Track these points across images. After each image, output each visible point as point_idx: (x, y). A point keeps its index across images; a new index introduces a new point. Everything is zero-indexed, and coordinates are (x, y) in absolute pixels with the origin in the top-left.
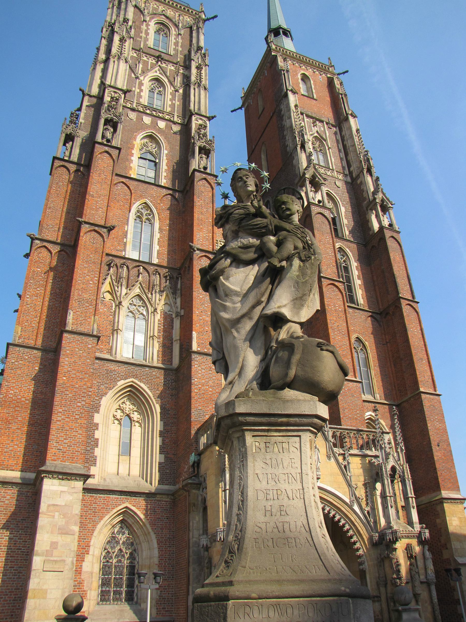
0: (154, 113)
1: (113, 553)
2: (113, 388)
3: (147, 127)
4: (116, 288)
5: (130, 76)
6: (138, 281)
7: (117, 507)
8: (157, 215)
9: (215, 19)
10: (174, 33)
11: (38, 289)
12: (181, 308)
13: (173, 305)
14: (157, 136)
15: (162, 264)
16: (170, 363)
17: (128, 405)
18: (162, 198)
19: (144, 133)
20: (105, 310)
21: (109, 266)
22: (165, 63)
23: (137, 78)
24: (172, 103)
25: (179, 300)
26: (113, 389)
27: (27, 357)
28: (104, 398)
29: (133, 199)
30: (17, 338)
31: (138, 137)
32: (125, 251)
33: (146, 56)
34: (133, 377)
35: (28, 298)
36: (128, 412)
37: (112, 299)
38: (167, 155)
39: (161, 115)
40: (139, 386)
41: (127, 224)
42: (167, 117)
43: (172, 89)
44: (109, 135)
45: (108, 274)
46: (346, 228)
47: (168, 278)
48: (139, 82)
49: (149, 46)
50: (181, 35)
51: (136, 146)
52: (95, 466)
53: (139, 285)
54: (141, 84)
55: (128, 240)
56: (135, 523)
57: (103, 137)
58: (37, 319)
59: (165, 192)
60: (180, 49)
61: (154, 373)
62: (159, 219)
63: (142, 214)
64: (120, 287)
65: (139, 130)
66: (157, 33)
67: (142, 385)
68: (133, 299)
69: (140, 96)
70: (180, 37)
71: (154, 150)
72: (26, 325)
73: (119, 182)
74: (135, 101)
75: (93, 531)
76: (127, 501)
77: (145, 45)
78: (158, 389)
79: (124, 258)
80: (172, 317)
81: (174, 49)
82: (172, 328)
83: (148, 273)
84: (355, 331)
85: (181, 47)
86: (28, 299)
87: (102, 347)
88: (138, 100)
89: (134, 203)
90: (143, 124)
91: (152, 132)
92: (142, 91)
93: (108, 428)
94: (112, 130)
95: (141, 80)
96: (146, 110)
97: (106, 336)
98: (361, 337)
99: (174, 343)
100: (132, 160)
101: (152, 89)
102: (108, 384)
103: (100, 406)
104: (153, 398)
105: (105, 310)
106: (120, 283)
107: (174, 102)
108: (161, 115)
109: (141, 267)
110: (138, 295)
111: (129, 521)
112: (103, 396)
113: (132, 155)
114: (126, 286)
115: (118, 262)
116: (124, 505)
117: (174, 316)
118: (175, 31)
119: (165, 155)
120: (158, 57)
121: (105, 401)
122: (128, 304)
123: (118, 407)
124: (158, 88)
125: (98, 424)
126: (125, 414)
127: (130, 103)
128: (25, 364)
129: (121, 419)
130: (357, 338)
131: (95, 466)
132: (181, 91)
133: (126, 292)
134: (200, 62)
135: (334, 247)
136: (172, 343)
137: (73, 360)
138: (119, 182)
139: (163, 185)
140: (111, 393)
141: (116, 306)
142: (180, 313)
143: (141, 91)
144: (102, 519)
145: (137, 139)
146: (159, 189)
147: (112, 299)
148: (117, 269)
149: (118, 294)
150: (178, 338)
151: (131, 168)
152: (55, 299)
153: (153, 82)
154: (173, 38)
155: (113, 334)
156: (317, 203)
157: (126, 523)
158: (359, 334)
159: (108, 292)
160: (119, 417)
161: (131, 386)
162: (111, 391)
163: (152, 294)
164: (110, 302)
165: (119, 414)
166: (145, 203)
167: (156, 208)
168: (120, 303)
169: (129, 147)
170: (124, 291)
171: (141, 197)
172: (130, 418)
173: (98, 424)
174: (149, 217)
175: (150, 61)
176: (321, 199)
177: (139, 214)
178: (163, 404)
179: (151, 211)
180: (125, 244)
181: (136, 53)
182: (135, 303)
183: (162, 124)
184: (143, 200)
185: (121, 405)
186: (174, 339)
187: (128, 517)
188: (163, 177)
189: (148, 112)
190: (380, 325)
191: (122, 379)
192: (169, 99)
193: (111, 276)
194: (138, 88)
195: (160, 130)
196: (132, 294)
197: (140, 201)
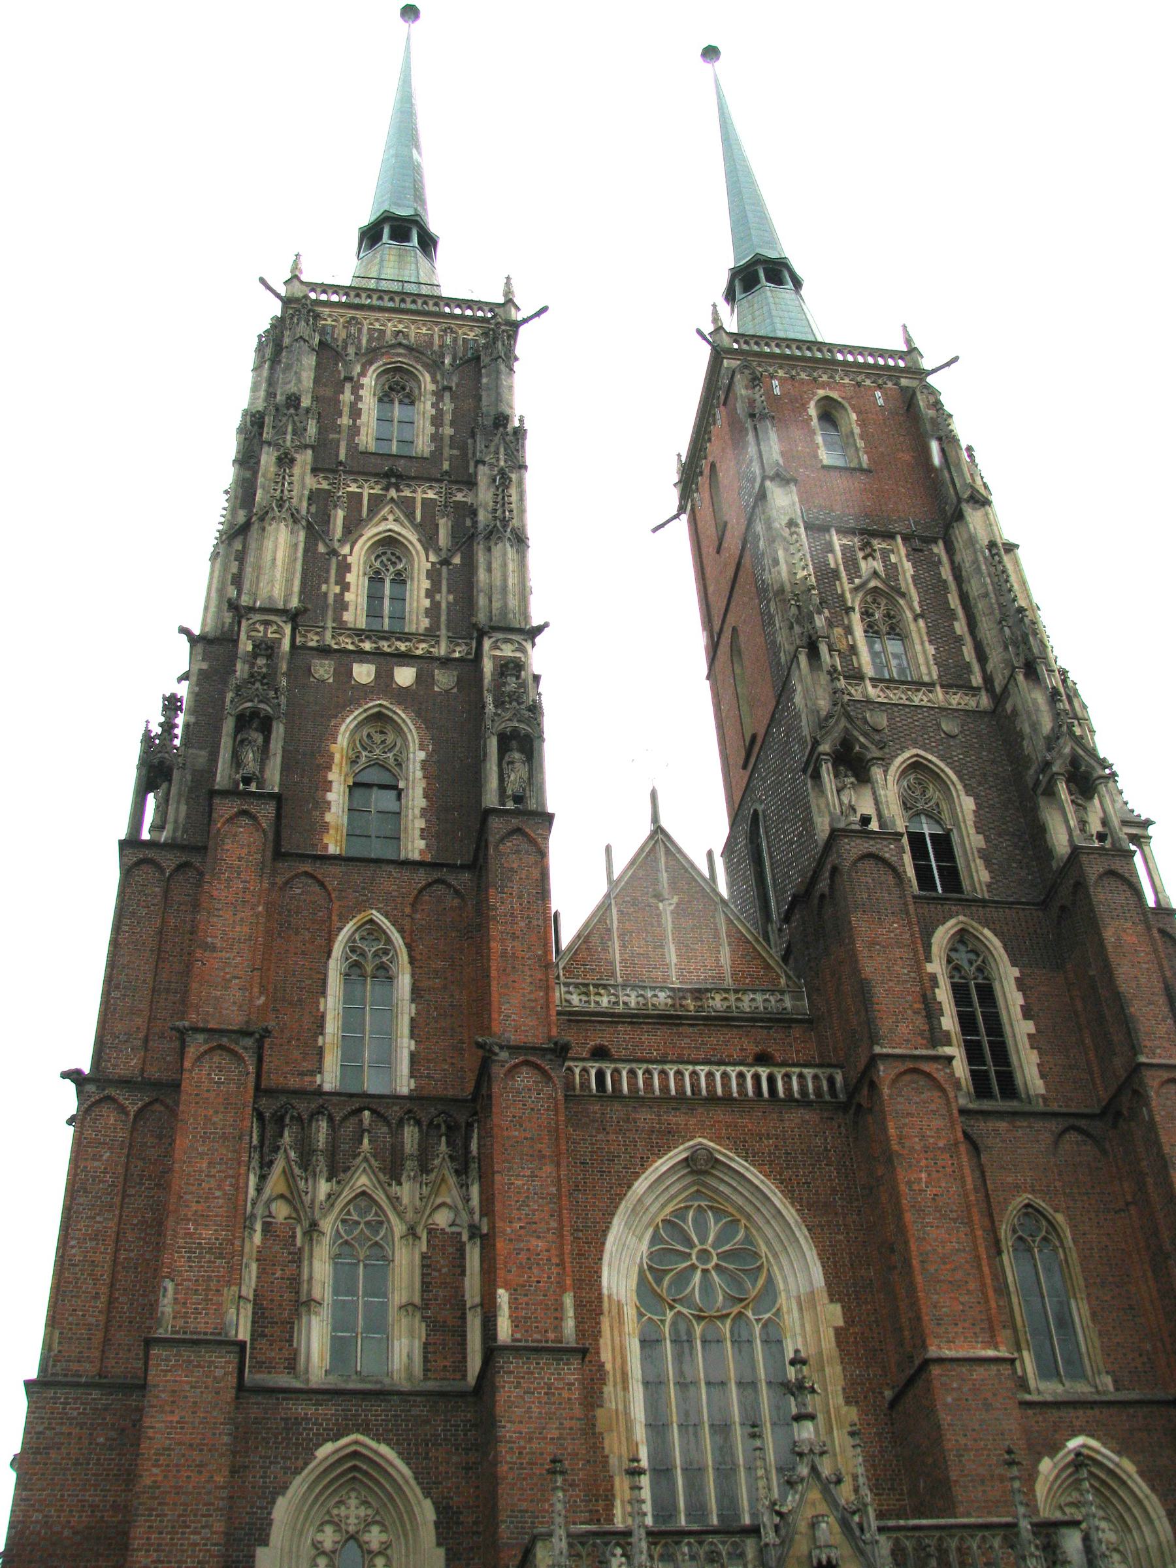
0: (385, 646)
2: (303, 1469)
3: (365, 691)
4: (302, 1184)
5: (310, 549)
6: (359, 1153)
9: (543, 316)
10: (431, 387)
11: (98, 1219)
12: (482, 1215)
13: (460, 1206)
14: (395, 713)
15: (425, 1093)
16: (458, 1375)
18: (416, 897)
19: (356, 713)
20: (277, 1248)
21: (279, 1121)
22: (409, 486)
23: (334, 553)
24: (432, 602)
25: (475, 1190)
26: (306, 1472)
27: (75, 1413)
29: (335, 918)
30: (51, 1363)
31: (343, 727)
32: (320, 1070)
33: (355, 481)
34: (358, 1431)
35: (73, 1247)
36: (352, 1529)
37: (294, 1215)
38: (423, 762)
40: (376, 1452)
42: (421, 649)
43: (432, 558)
45: (278, 1148)
47: (443, 1129)
48: (339, 565)
49: (361, 448)
50: (449, 388)
53: (365, 1165)
54: (344, 567)
55: (329, 1039)
58: (101, 1304)
59: (422, 877)
60: (448, 431)
61: (415, 1411)
62: (412, 960)
63: (363, 954)
64: (310, 1182)
66: (386, 399)
67: (384, 1449)
68: (351, 1207)
69: (342, 605)
70: (447, 395)
71: (390, 755)
72: (71, 1324)
73: (297, 876)
74: (330, 624)
77: (352, 448)
78: (427, 1454)
79: (319, 1092)
80: (460, 1241)
81: (436, 438)
82: (463, 1273)
83: (389, 1124)
84: (1018, 1188)
85: (452, 424)
86: (74, 1251)
87: (273, 1354)
88: (338, 619)
89: (340, 929)
91: (380, 705)
92: (348, 590)
95: (345, 556)
96: (362, 641)
97: (282, 1323)
98: (1041, 1203)
99: (469, 1316)
100: (329, 803)
101: (377, 572)
102: (290, 1458)
103: (270, 1524)
104: (413, 1482)
105: (277, 1248)
106: (311, 1168)
107: (438, 597)
108: (403, 647)
109: (367, 1113)
110: (363, 1193)
112: (278, 1494)
113: (328, 786)
114: (325, 1174)
115: (303, 1107)
117: (465, 1238)
118: (434, 381)
119: (418, 767)
120: (386, 475)
121: (282, 1510)
122: (339, 1223)
124: (394, 564)
126: (345, 1536)
127: (317, 633)
128: (70, 1434)
129: (334, 1552)
130: (1028, 1206)
132: (457, 560)
133: (328, 1191)
134: (502, 463)
136: (463, 1317)
138: (297, 876)
139: (416, 856)
140: (298, 1485)
141: (304, 1234)
142: (479, 1228)
143: (346, 587)
145: (340, 738)
146: (407, 873)
147: (294, 1215)
148: (303, 1129)
149: (307, 1199)
150: (477, 1300)
151: (325, 827)
152: (144, 1239)
153: (380, 550)
154: (429, 404)
155: (299, 1317)
158: (1033, 1192)
160: (328, 1545)
161: (355, 1454)
162: (299, 1479)
163: (400, 1184)
164: (287, 1224)
167: (401, 931)
168: (314, 1225)
169: (318, 766)
171: (360, 907)
172: (360, 1546)
174: (384, 959)
175: (366, 493)
178: (443, 1498)
179: (389, 941)
180: (320, 1052)
181: (326, 478)
182: (356, 1218)
183: (405, 676)
184: (363, 914)
186: (468, 1305)
189: (367, 646)
190: (1104, 1152)
191: (326, 1441)
192: (423, 593)
193: (285, 1150)
194: (337, 583)
195: (402, 696)
196: (347, 1195)
197: (355, 920)
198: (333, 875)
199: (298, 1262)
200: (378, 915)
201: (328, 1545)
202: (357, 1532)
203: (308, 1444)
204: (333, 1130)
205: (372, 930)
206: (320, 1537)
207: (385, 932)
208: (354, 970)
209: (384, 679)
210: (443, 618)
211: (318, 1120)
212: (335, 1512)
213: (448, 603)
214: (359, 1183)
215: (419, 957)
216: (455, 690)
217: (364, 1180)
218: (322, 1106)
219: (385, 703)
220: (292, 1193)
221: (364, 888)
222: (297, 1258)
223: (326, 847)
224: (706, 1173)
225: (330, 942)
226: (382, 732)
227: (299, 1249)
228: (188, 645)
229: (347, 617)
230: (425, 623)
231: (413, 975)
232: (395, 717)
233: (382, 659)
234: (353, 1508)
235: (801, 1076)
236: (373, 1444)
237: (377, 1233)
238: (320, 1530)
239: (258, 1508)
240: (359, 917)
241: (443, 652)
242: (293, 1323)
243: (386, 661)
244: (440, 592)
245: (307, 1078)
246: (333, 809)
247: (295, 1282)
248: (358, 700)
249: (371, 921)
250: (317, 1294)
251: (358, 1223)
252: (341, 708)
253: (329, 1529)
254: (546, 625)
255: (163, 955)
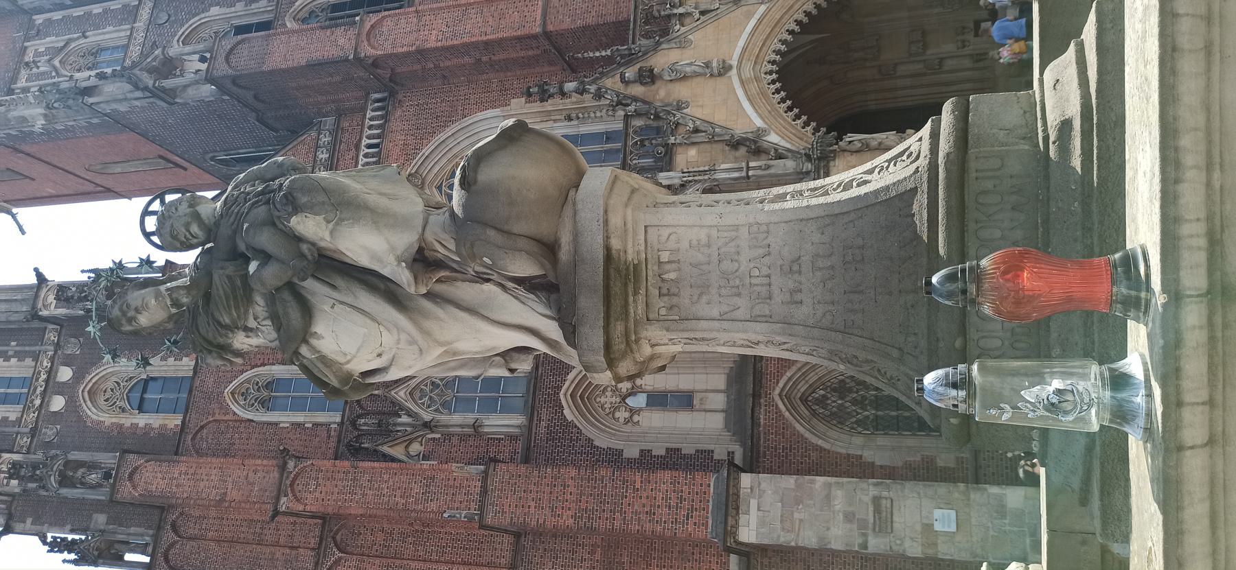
1: (858, 414)
2: (579, 429)
3: (72, 403)
7: (780, 411)
8: (255, 370)
17: (606, 400)
19: (85, 408)
28: (596, 443)
29: (227, 417)
31: (94, 417)
32: (328, 425)
34: (558, 394)
36: (618, 400)
37: (420, 439)
39: (43, 377)
41: (276, 424)
42: (46, 363)
44: (94, 477)
45: (375, 450)
46: (253, 6)
51: (114, 420)
52: (712, 451)
53: (393, 393)
56: (807, 379)
57: (99, 486)
62: (263, 365)
65: (80, 417)
74: (16, 429)
75: (821, 449)
76: (770, 394)
79: (341, 424)
88: (14, 424)
89: (235, 414)
90: (66, 411)
91: (83, 391)
93: (647, 433)
94: (82, 470)
96: (34, 406)
107: (10, 353)
111: (802, 390)
116: (777, 399)
121: (602, 441)
123: (611, 416)
125: (642, 451)
129: (631, 410)
131: (712, 451)
135: (294, 32)
137: (533, 504)
141: (433, 432)
144: (802, 436)
147: (420, 439)
148: (364, 435)
156: (206, 64)
157: (807, 395)
159: (407, 447)
160: (627, 415)
165: (622, 415)
166: (233, 393)
169: (119, 433)
170: (404, 419)
173: (642, 451)
176: (197, 57)
177: (256, 404)
179: (248, 381)
180: (316, 425)
183: (65, 374)
184: (227, 398)
185: (607, 410)
187: (796, 390)
188: (178, 363)
191: (563, 413)
195: (78, 377)
197: (230, 404)
198: (195, 420)
199: (450, 435)
200: (229, 388)
201: (627, 415)
202: (621, 396)
203: (564, 426)
204: (368, 414)
205: (241, 394)
206: (622, 420)
207: (242, 383)
208: (267, 404)
209: (64, 389)
210: (27, 348)
211: (360, 425)
212: (607, 410)
213: (17, 345)
214: (403, 396)
215: (261, 361)
216: (81, 339)
217: (402, 393)
218: (351, 422)
219: (82, 388)
220: (405, 441)
221: (209, 399)
222: (448, 437)
223: (176, 426)
224: (424, 180)
225: (242, 421)
226: (105, 391)
227: (442, 435)
228: (11, 535)
229: (13, 417)
230: (29, 362)
231: (273, 364)
232: (94, 381)
233: (49, 391)
234: (606, 400)
235: (371, 119)
236: (567, 384)
237: (439, 385)
238: (617, 420)
239: (600, 457)
240: (228, 401)
241: (52, 348)
242: (488, 438)
243: (52, 386)
244: (7, 352)
245: (332, 433)
246: (151, 422)
247: (463, 438)
248: (76, 406)
249: (233, 393)
250: (472, 421)
251: (431, 398)
252: (81, 419)
253: (617, 415)
254: (36, 270)
255: (235, 539)
